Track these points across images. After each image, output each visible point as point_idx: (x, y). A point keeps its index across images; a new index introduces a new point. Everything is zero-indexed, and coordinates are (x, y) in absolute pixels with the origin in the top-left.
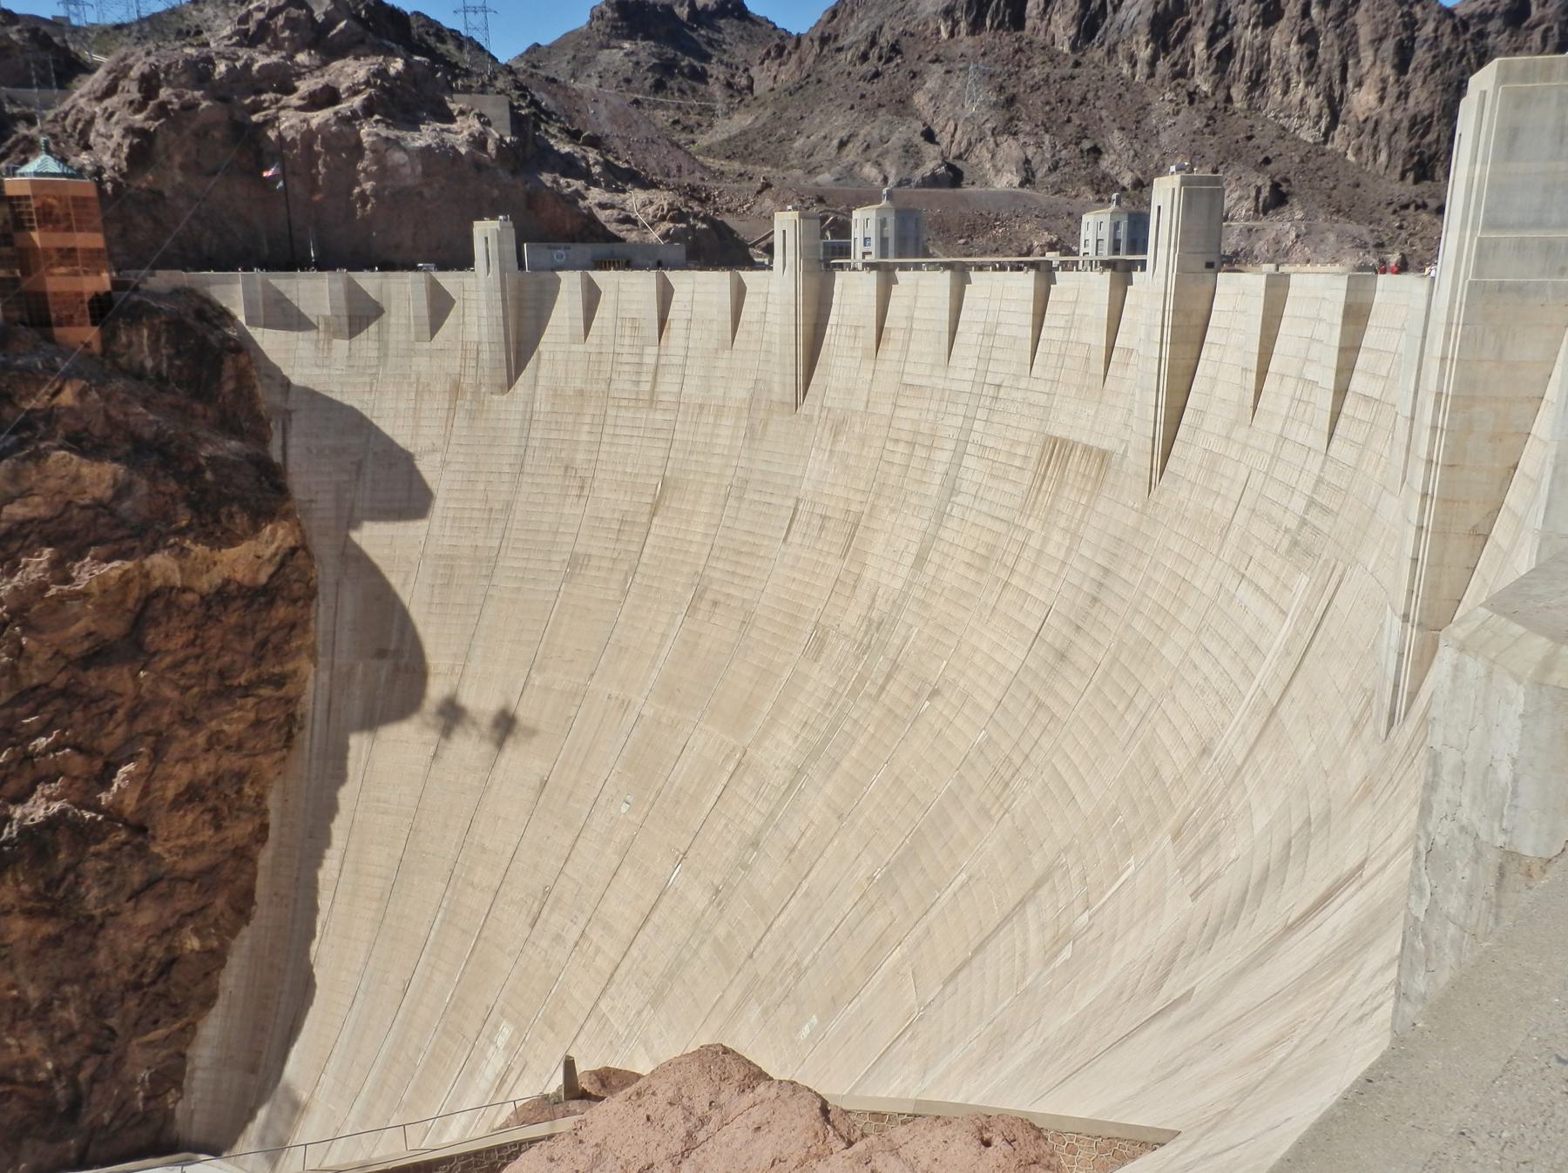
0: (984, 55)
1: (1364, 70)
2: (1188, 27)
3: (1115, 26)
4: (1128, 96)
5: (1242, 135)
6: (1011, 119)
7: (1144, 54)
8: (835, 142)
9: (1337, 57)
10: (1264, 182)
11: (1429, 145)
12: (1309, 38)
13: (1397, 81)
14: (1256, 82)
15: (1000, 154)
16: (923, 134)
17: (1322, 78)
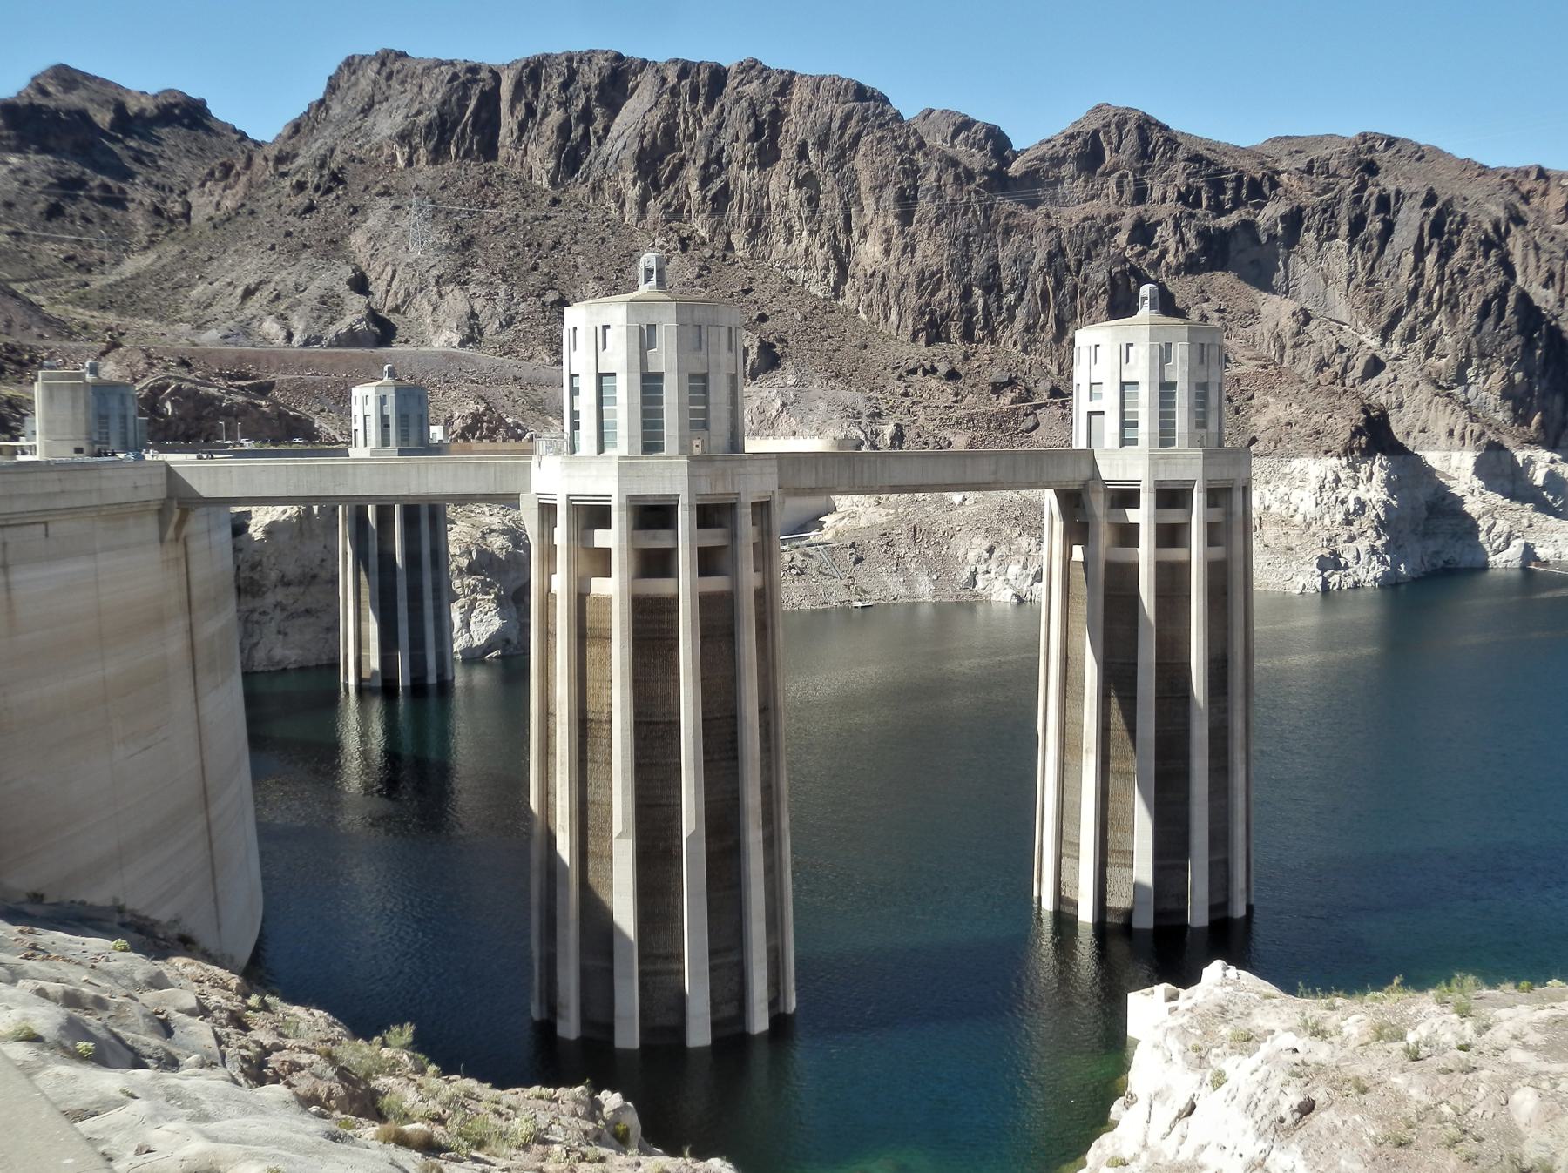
0: (443, 188)
1: (868, 220)
2: (682, 163)
3: (600, 159)
4: (613, 240)
5: (738, 288)
6: (464, 265)
7: (633, 193)
8: (240, 291)
9: (839, 204)
10: (751, 341)
11: (941, 303)
12: (807, 182)
13: (902, 232)
14: (757, 230)
15: (444, 306)
16: (349, 282)
17: (824, 227)
